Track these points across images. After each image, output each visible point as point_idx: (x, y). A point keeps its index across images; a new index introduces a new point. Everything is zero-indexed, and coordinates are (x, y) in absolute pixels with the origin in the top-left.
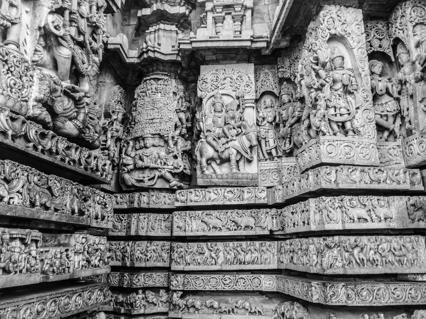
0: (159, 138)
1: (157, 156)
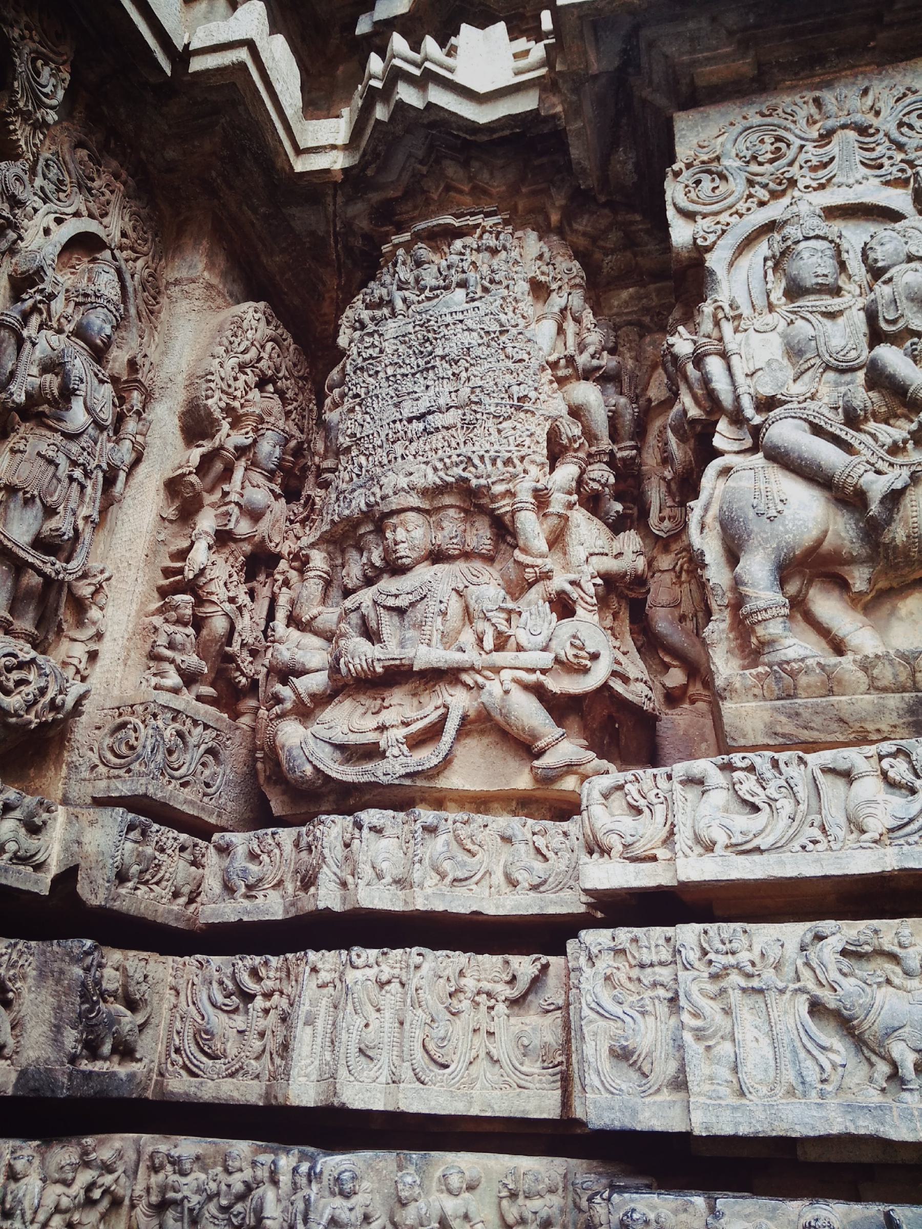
0: (466, 511)
1: (455, 606)
